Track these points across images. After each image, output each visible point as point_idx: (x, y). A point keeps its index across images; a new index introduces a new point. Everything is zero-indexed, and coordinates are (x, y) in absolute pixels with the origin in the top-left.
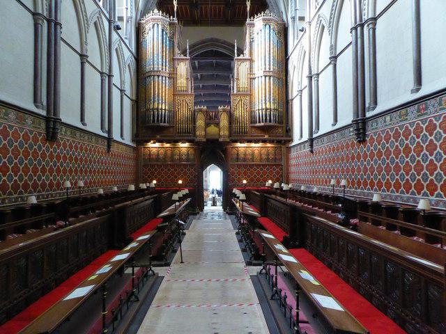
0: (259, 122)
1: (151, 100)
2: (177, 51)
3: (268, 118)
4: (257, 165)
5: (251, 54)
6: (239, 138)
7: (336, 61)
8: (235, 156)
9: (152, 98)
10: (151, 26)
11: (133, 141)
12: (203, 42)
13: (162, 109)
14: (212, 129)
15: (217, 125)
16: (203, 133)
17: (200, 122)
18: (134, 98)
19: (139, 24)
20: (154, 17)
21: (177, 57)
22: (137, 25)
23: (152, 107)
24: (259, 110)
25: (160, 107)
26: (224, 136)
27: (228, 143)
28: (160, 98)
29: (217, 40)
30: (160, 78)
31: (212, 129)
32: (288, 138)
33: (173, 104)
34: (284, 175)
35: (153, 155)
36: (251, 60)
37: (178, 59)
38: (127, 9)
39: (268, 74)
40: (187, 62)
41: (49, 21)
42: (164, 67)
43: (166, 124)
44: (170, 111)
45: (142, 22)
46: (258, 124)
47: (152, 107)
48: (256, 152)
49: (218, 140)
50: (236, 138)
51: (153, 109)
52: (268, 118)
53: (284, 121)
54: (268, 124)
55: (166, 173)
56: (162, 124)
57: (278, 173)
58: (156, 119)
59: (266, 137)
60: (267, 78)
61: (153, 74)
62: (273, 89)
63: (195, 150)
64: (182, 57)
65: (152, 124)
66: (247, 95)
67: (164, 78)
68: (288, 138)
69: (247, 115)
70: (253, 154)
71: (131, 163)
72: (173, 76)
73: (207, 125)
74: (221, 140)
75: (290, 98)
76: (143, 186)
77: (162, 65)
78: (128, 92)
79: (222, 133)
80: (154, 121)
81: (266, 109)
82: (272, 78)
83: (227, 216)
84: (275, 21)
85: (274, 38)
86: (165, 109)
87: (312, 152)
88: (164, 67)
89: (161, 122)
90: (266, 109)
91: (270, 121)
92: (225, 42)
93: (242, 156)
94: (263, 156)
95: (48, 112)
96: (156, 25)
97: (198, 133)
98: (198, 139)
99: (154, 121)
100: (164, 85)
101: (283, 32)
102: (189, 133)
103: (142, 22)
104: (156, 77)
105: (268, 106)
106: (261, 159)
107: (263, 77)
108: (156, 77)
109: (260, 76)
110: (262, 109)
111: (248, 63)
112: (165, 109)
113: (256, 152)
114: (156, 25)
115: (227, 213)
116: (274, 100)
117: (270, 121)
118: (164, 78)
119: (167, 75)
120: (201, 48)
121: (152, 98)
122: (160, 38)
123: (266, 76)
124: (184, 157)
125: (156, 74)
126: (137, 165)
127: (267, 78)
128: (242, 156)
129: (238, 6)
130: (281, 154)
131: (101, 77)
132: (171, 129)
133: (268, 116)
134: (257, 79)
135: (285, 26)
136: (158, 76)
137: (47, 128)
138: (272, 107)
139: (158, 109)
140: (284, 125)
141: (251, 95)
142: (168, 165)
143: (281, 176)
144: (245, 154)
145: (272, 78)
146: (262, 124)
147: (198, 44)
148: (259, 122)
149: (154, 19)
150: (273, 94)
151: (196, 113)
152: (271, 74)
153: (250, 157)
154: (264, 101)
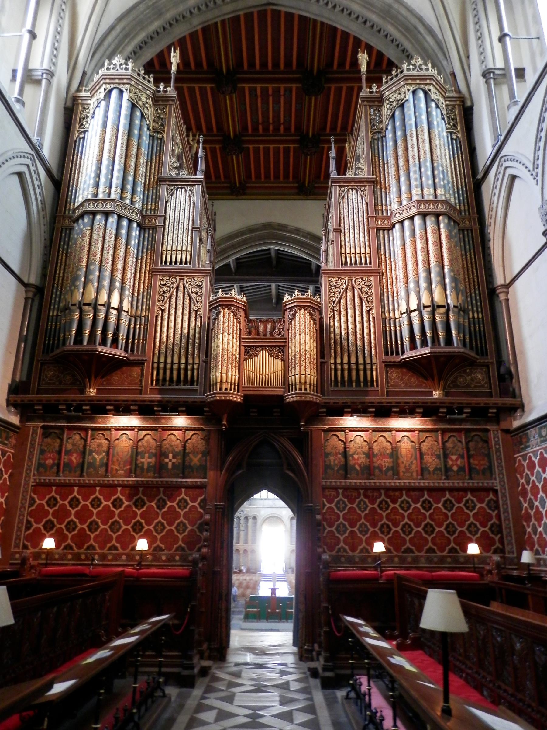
0: (413, 347)
1: (77, 278)
4: (410, 490)
6: (348, 399)
8: (336, 461)
9: (82, 273)
12: (251, 230)
13: (108, 305)
16: (233, 375)
18: (33, 279)
19: (75, 99)
20: (112, 72)
21: (168, 173)
22: (69, 104)
24: (409, 312)
25: (103, 298)
28: (107, 273)
29: (283, 227)
34: (508, 525)
35: (68, 453)
37: (172, 182)
38: (33, 35)
39: (431, 208)
40: (198, 189)
43: (119, 353)
44: (135, 317)
48: (405, 446)
50: (341, 399)
53: (491, 347)
55: (107, 514)
56: (107, 350)
57: (484, 518)
59: (436, 394)
61: (91, 208)
63: (207, 439)
66: (369, 273)
68: (508, 401)
70: (395, 453)
74: (291, 398)
75: (499, 280)
86: (120, 309)
89: (104, 343)
90: (434, 307)
92: (297, 231)
93: (359, 459)
94: (428, 459)
96: (115, 93)
97: (217, 374)
102: (192, 384)
103: (83, 94)
105: (437, 297)
106: (423, 471)
107: (417, 220)
109: (406, 214)
112: (120, 309)
113: (405, 446)
114: (115, 93)
115: (314, 673)
118: (125, 223)
120: (244, 242)
121: (82, 273)
122: (123, 122)
123: (424, 216)
124: (170, 461)
125: (100, 208)
128: (359, 459)
129: (333, 86)
130: (489, 455)
132: (136, 371)
133: (440, 327)
134: (397, 226)
135: (462, 100)
139: (95, 306)
140: (491, 359)
141: (380, 274)
142: (113, 487)
144: (370, 454)
149: (112, 78)
152: (441, 208)
153: (386, 463)
154: (423, 284)
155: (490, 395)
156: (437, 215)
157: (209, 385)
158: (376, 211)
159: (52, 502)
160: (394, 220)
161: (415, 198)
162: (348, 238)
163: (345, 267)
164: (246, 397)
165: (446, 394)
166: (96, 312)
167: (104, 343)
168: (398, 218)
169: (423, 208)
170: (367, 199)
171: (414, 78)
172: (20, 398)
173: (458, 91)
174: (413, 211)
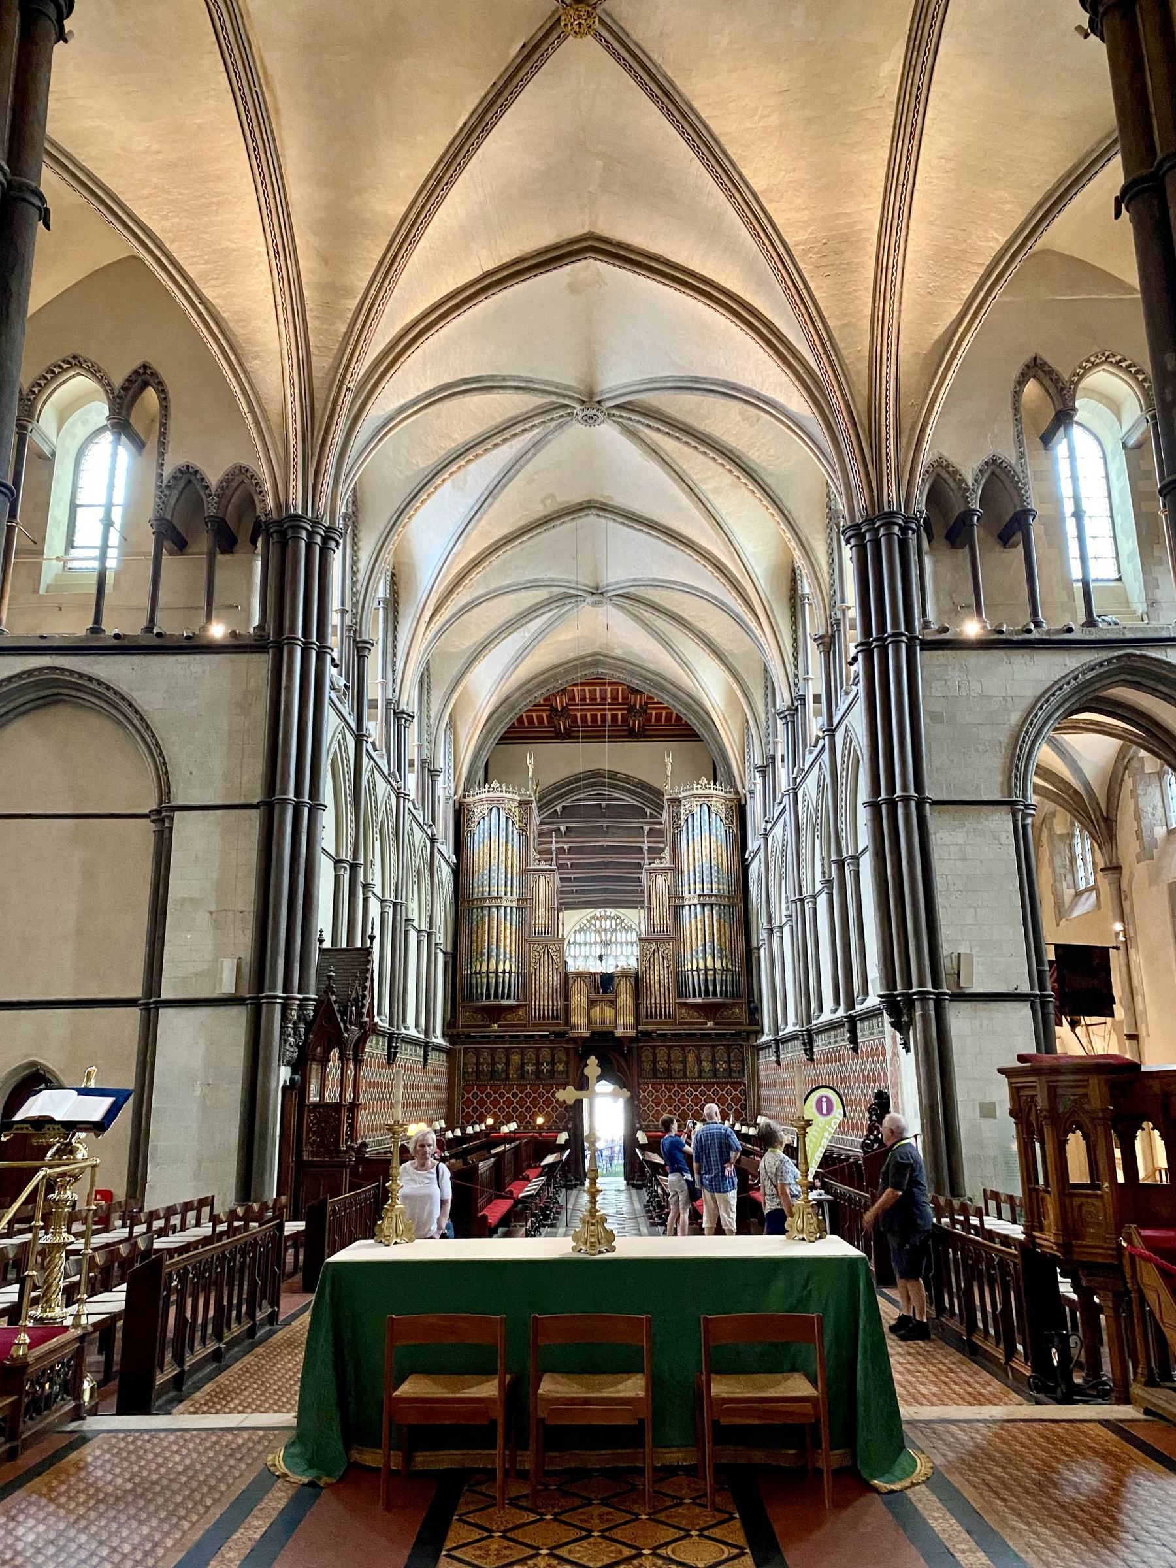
0: (694, 996)
1: (482, 954)
2: (534, 855)
3: (711, 988)
5: (676, 856)
7: (815, 903)
9: (486, 951)
10: (486, 812)
11: (444, 1035)
13: (504, 972)
14: (603, 1013)
15: (612, 1003)
16: (585, 1020)
17: (579, 999)
18: (449, 949)
20: (491, 794)
22: (457, 806)
23: (484, 969)
25: (501, 969)
26: (626, 1027)
27: (631, 1039)
30: (502, 911)
31: (603, 1013)
32: (754, 1028)
33: (524, 958)
36: (676, 871)
39: (707, 901)
41: (395, 904)
42: (509, 889)
43: (512, 1002)
45: (467, 800)
46: (691, 1000)
47: (484, 969)
49: (612, 1033)
51: (488, 972)
52: (711, 988)
54: (711, 999)
56: (505, 1002)
58: (492, 991)
60: (707, 909)
61: (488, 903)
62: (719, 930)
64: (543, 866)
65: (485, 1003)
67: (509, 910)
68: (754, 1028)
69: (669, 981)
71: (443, 1082)
72: (525, 908)
73: (592, 1003)
74: (618, 1034)
75: (754, 944)
76: (470, 1130)
77: (506, 886)
78: (440, 937)
79: (620, 1020)
80: (488, 996)
81: (706, 969)
82: (716, 909)
83: (634, 1191)
84: (720, 797)
85: (720, 829)
87: (778, 1062)
88: (509, 889)
89: (503, 997)
90: (706, 969)
91: (715, 994)
95: (391, 1024)
96: (494, 811)
97: (574, 1020)
98: (574, 1033)
99: (488, 996)
100: (508, 925)
101: (738, 813)
103: (467, 800)
104: (494, 910)
105: (709, 964)
108: (494, 910)
109: (691, 902)
110: (698, 970)
111: (670, 875)
112: (510, 972)
114: (494, 811)
116: (721, 951)
117: (715, 994)
118: (509, 910)
119: (515, 904)
123: (703, 905)
125: (494, 903)
126: (450, 1087)
127: (707, 909)
131: (382, 908)
136: (498, 907)
137: (390, 1047)
138: (718, 966)
139: (497, 972)
140: (745, 999)
143: (744, 1107)
145: (716, 909)
146: (699, 1000)
147: (570, 783)
148: (694, 996)
150: (720, 939)
151: (571, 981)
152: (713, 900)
155: (741, 1024)
156: (712, 905)
157: (568, 1023)
158: (675, 892)
159: (475, 1095)
160: (687, 902)
161: (698, 892)
162: (656, 913)
163: (654, 935)
164: (593, 1033)
165: (716, 1024)
166: (497, 976)
167: (503, 997)
168: (687, 902)
169: (702, 900)
170: (668, 882)
171: (700, 796)
172: (450, 1031)
173: (737, 793)
174: (696, 901)
